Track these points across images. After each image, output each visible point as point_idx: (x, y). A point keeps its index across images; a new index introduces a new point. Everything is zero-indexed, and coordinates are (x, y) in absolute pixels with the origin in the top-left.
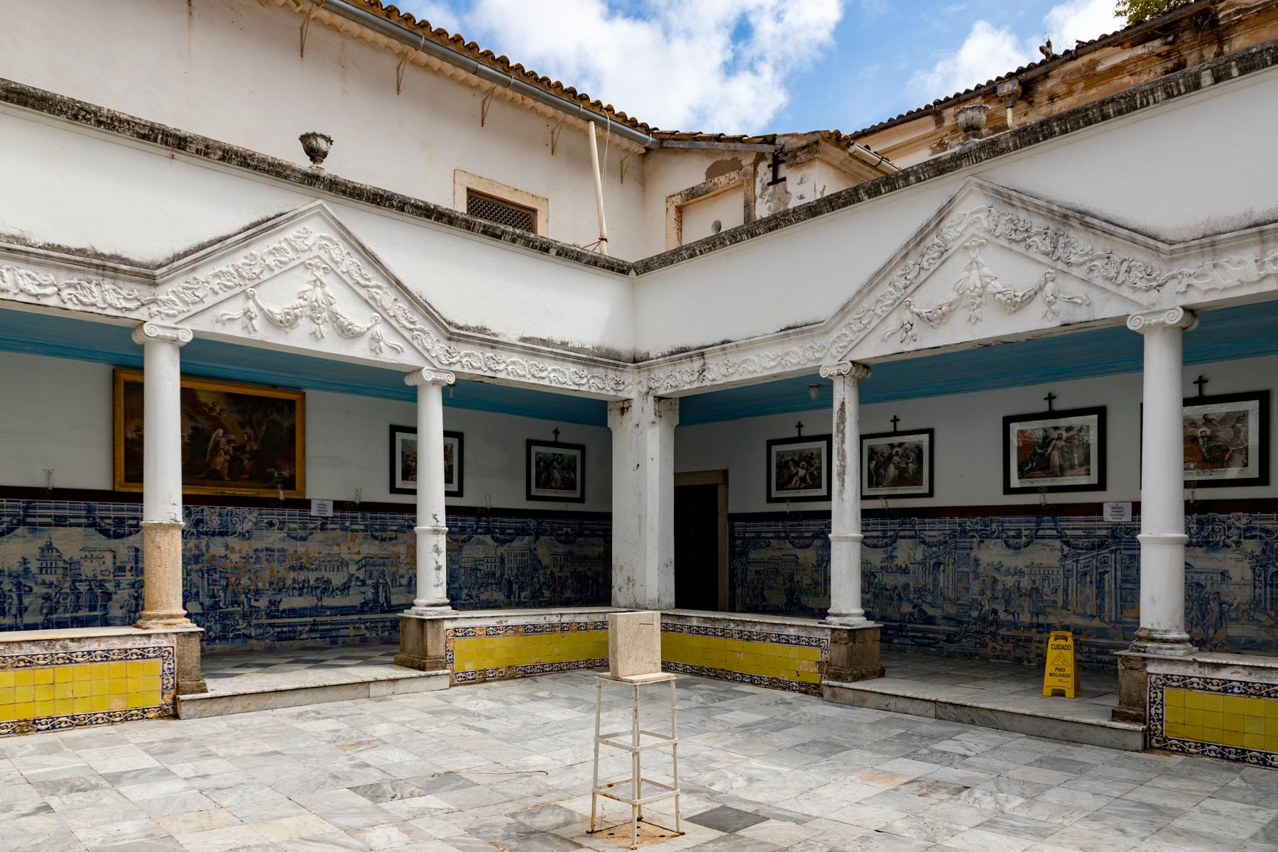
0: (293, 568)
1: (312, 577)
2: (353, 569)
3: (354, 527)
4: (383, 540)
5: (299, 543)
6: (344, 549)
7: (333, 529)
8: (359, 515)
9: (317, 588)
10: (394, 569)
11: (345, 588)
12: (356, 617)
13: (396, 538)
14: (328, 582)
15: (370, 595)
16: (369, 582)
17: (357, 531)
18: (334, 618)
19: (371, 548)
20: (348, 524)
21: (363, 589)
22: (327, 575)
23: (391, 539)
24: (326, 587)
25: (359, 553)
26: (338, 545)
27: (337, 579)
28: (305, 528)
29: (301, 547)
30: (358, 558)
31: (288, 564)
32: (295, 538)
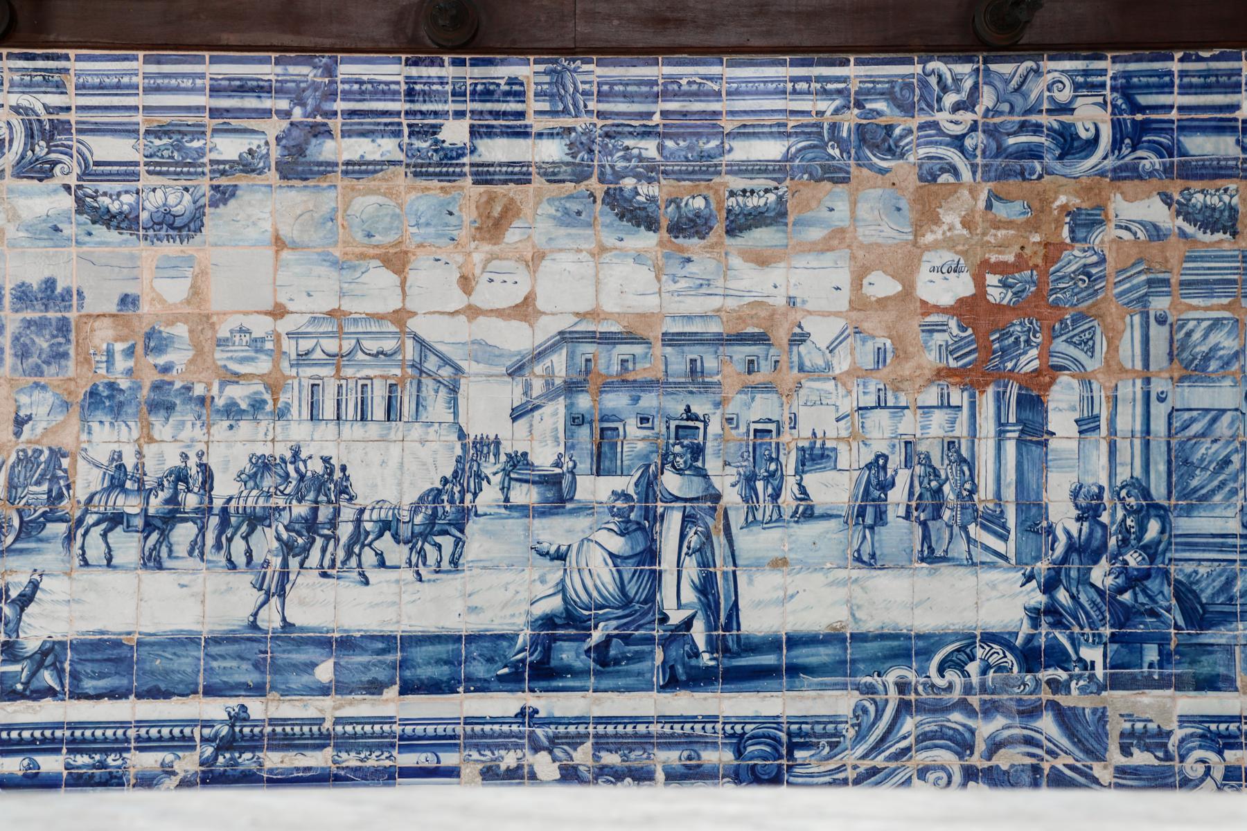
0: (103, 400)
1: (230, 453)
2: (486, 407)
3: (497, 150)
4: (690, 226)
5: (152, 253)
6: (432, 285)
7: (360, 169)
8: (526, 71)
9: (255, 520)
10: (762, 408)
11: (439, 523)
12: (503, 704)
13: (776, 216)
14: (332, 484)
15: (597, 574)
16: (595, 489)
17: (519, 174)
18: (363, 707)
19: (609, 278)
20: (455, 132)
21: (554, 532)
22: (319, 443)
23: (739, 223)
24: (313, 517)
25: (525, 310)
26: (397, 261)
27: (392, 469)
28: (188, 166)
29: (160, 278)
30: (517, 338)
31: (77, 376)
32: (124, 221)
